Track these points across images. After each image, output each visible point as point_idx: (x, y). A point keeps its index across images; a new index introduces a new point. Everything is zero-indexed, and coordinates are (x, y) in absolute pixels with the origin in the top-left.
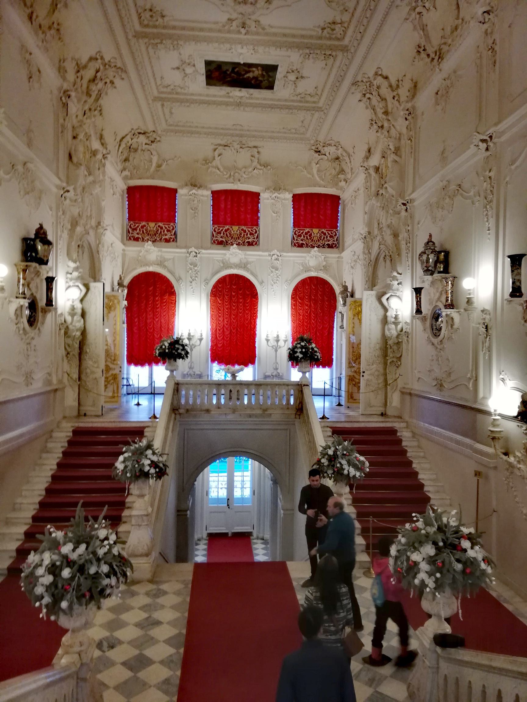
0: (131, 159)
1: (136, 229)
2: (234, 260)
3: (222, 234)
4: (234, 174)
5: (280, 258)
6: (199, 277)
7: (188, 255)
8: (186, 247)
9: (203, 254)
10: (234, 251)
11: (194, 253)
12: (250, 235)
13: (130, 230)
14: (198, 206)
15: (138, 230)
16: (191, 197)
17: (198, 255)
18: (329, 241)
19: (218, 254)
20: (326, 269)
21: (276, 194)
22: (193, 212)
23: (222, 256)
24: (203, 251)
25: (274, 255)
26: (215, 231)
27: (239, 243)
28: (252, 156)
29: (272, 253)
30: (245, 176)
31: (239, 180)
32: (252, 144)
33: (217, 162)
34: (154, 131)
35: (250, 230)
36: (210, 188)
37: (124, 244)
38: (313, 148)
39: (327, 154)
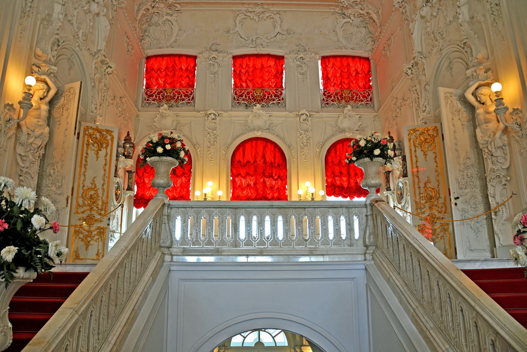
1: (152, 96)
2: (258, 122)
3: (244, 97)
4: (257, 38)
5: (310, 119)
7: (206, 118)
10: (258, 112)
11: (212, 115)
13: (146, 96)
15: (154, 97)
16: (210, 62)
17: (218, 118)
18: (362, 101)
19: (241, 114)
25: (302, 114)
30: (267, 41)
31: (262, 45)
35: (274, 92)
37: (139, 111)
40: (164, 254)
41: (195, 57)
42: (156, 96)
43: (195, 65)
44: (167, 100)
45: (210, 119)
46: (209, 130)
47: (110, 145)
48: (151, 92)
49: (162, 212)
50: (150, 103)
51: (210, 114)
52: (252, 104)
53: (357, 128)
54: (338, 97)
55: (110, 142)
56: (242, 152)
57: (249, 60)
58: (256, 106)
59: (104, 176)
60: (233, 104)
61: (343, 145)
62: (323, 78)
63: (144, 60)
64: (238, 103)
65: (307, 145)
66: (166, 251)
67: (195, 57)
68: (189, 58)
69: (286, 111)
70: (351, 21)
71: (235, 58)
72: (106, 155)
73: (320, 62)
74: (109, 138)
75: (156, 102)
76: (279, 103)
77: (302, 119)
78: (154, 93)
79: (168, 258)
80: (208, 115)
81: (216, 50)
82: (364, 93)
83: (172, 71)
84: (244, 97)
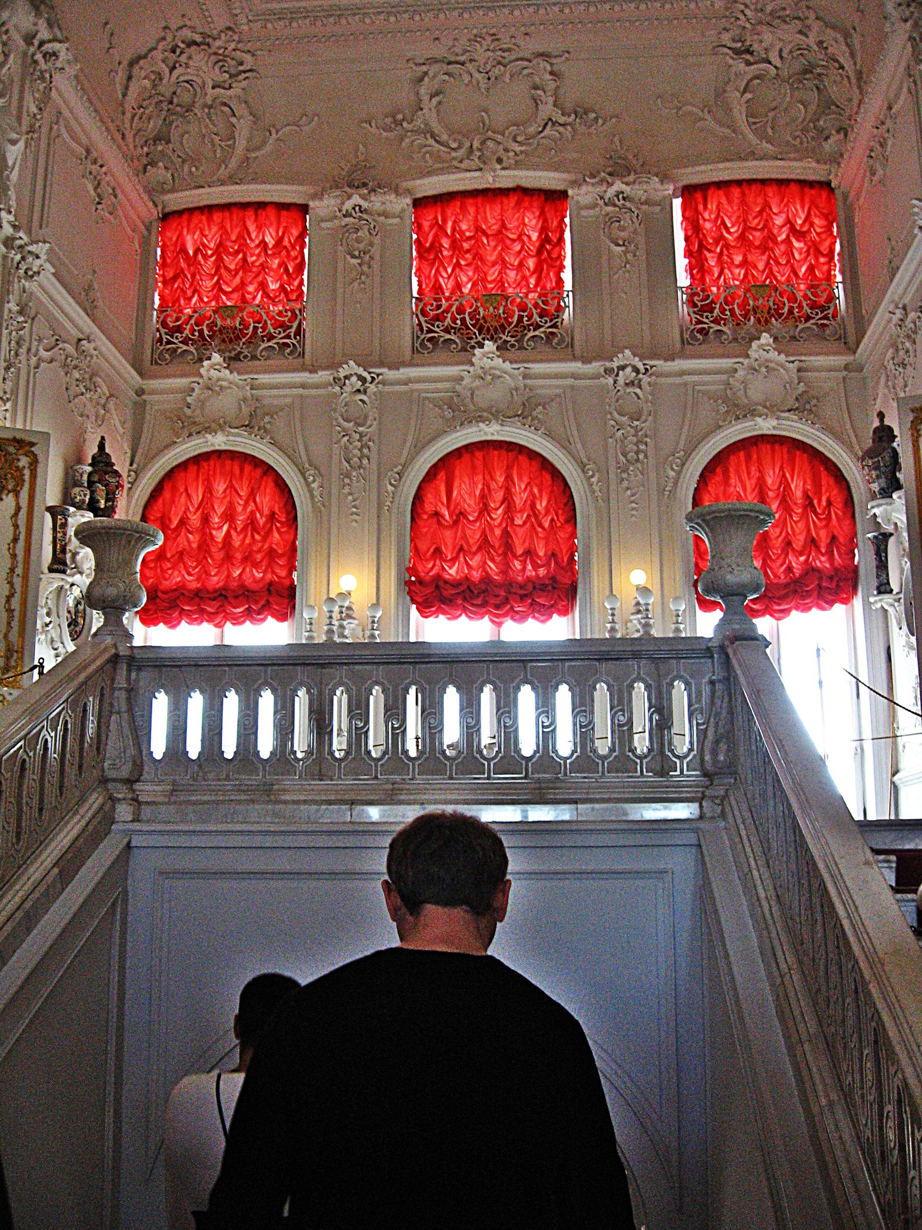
0: (174, 136)
1: (179, 329)
3: (448, 321)
4: (483, 143)
5: (645, 379)
6: (374, 460)
8: (334, 365)
9: (383, 383)
11: (354, 379)
12: (541, 316)
14: (371, 244)
17: (372, 388)
20: (805, 406)
21: (618, 186)
22: (355, 261)
23: (448, 385)
24: (389, 374)
25: (622, 368)
26: (424, 313)
27: (506, 342)
28: (536, 88)
29: (615, 365)
30: (518, 149)
31: (500, 161)
32: (530, 46)
33: (429, 115)
34: (229, 28)
36: (409, 191)
38: (726, 38)
39: (774, 57)
40: (113, 800)
41: (304, 209)
42: (192, 331)
43: (303, 233)
44: (224, 341)
45: (347, 389)
46: (346, 424)
47: (27, 486)
48: (178, 319)
49: (113, 680)
50: (175, 350)
51: (346, 377)
52: (473, 342)
53: (791, 403)
54: (732, 311)
55: (27, 472)
56: (443, 488)
57: (464, 209)
58: (481, 346)
59: (12, 570)
60: (417, 345)
61: (748, 458)
62: (688, 253)
63: (157, 227)
64: (431, 340)
65: (638, 460)
66: (121, 792)
67: (304, 209)
68: (285, 213)
69: (575, 358)
70: (773, 72)
71: (419, 204)
72: (16, 515)
73: (677, 203)
74: (24, 461)
75: (192, 349)
76: (552, 334)
77: (621, 380)
78: (187, 322)
79: (124, 812)
80: (340, 382)
81: (365, 185)
82: (813, 294)
83: (237, 252)
84: (448, 321)
